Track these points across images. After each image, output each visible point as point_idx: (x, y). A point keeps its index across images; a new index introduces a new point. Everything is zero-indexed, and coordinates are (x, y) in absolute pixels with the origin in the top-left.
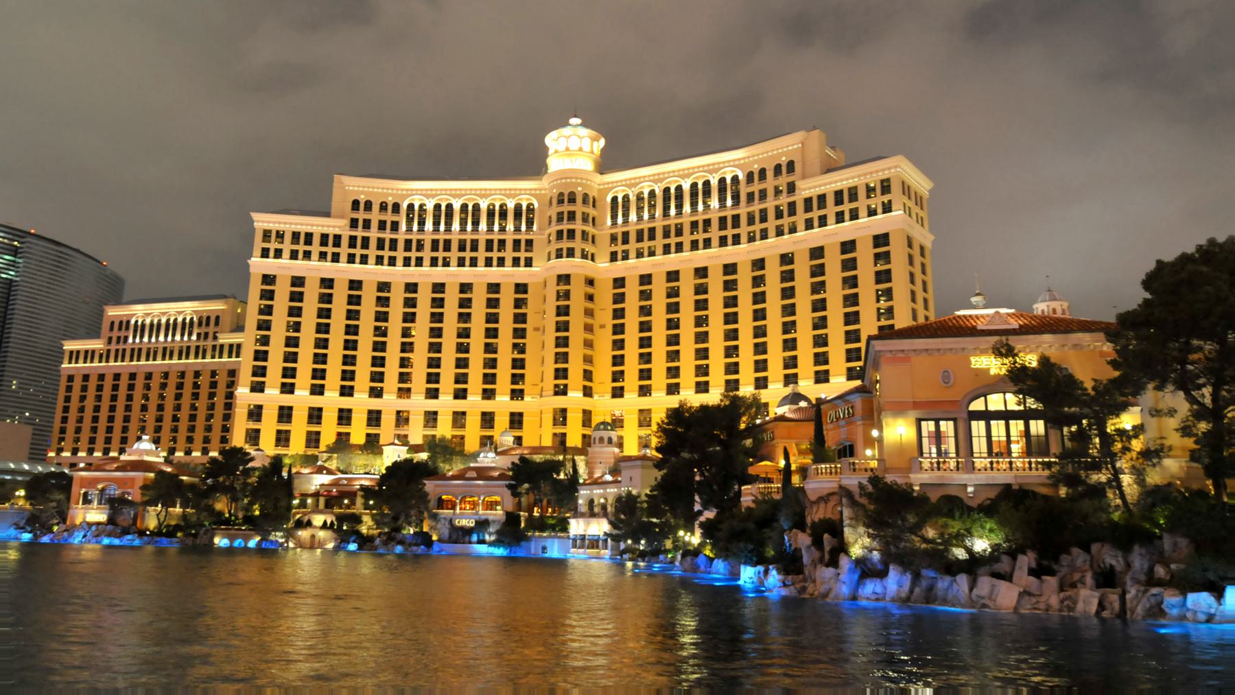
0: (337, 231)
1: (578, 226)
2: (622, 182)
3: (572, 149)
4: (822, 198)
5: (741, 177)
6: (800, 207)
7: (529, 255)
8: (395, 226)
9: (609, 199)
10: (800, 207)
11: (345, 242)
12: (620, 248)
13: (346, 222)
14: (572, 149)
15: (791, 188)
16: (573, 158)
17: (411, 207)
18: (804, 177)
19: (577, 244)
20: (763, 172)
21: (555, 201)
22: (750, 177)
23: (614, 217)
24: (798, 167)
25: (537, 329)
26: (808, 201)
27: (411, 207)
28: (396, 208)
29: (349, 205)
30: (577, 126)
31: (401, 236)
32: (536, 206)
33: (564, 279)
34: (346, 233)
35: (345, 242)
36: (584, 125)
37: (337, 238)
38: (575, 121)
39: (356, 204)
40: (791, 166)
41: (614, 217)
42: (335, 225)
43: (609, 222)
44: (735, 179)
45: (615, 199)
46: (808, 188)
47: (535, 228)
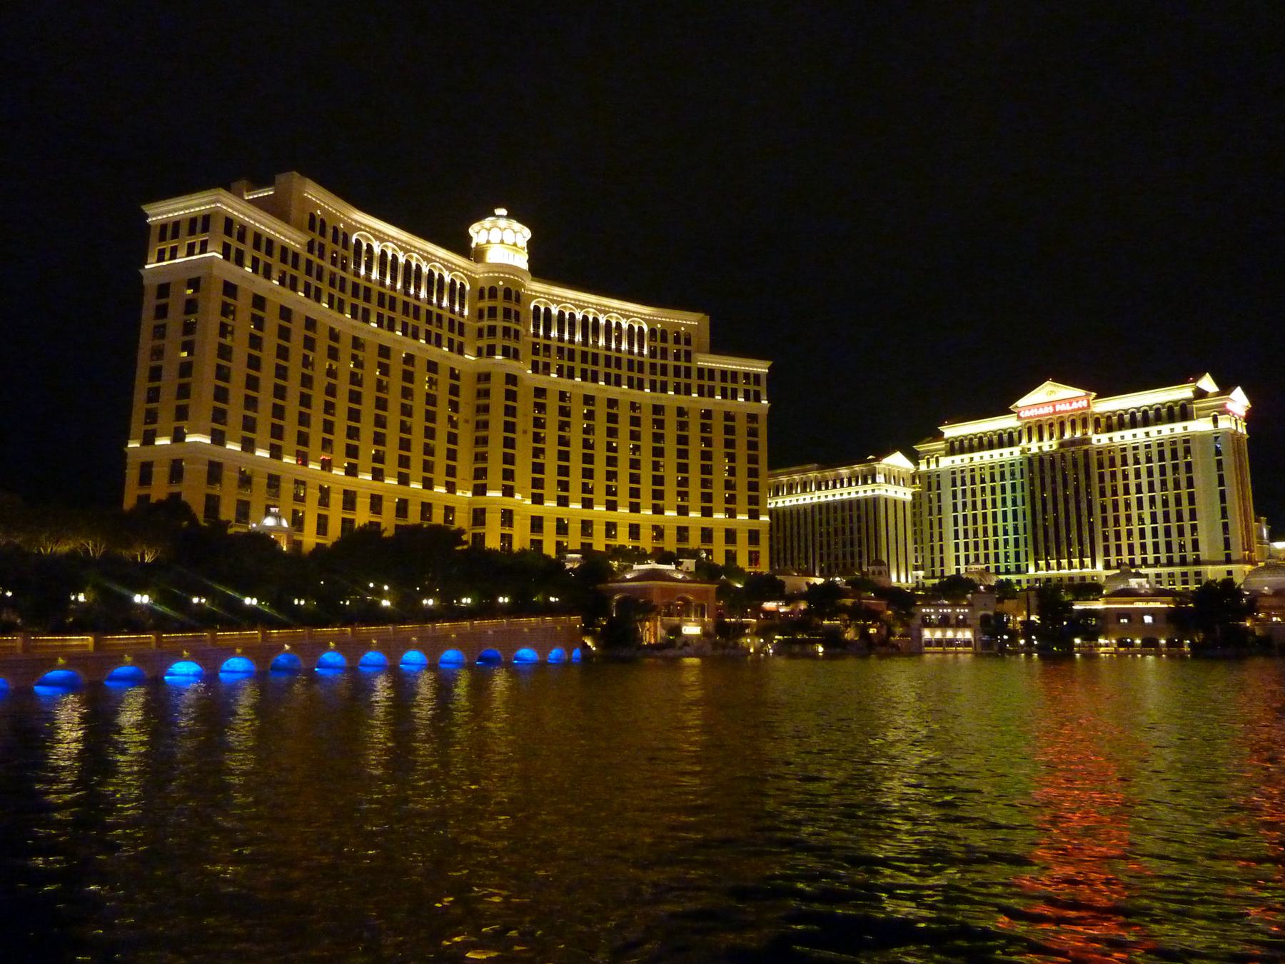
1: (500, 323)
2: (543, 294)
3: (503, 241)
4: (711, 371)
6: (694, 374)
7: (461, 339)
9: (532, 308)
10: (694, 374)
12: (541, 359)
13: (305, 239)
14: (503, 241)
15: (688, 356)
17: (358, 242)
18: (700, 351)
19: (499, 341)
20: (664, 333)
21: (500, 294)
22: (653, 332)
23: (536, 327)
24: (694, 340)
25: (467, 421)
26: (701, 370)
28: (346, 238)
29: (307, 218)
30: (499, 217)
32: (468, 288)
33: (511, 379)
34: (305, 255)
35: (302, 265)
36: (509, 216)
37: (296, 256)
38: (501, 211)
41: (536, 327)
42: (293, 239)
43: (532, 330)
44: (641, 329)
45: (537, 309)
46: (706, 361)
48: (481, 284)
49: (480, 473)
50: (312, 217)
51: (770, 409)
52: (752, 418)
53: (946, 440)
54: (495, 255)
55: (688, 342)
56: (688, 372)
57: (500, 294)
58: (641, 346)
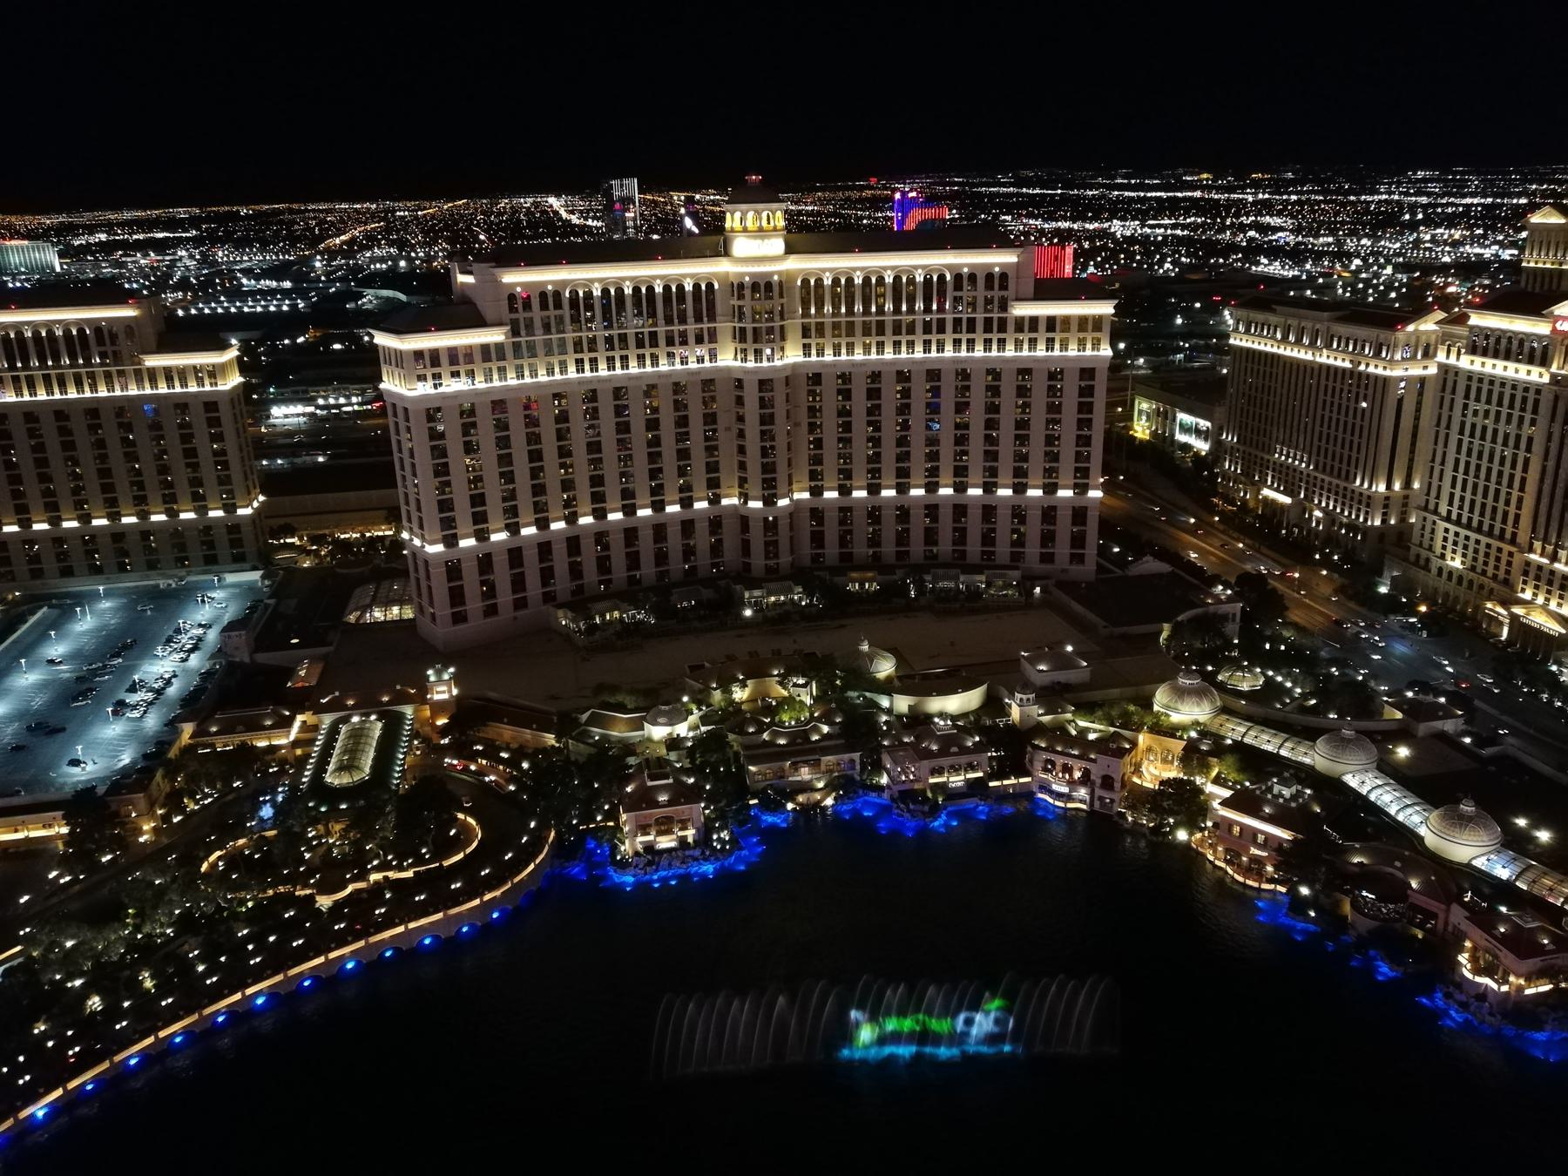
4: (1034, 321)
5: (948, 277)
10: (1011, 327)
15: (1004, 307)
18: (1018, 299)
20: (972, 277)
21: (747, 292)
22: (958, 278)
25: (728, 429)
40: (1004, 276)
46: (1022, 310)
50: (512, 298)
51: (1113, 357)
52: (1087, 373)
53: (1472, 328)
54: (742, 246)
55: (1004, 286)
57: (747, 292)
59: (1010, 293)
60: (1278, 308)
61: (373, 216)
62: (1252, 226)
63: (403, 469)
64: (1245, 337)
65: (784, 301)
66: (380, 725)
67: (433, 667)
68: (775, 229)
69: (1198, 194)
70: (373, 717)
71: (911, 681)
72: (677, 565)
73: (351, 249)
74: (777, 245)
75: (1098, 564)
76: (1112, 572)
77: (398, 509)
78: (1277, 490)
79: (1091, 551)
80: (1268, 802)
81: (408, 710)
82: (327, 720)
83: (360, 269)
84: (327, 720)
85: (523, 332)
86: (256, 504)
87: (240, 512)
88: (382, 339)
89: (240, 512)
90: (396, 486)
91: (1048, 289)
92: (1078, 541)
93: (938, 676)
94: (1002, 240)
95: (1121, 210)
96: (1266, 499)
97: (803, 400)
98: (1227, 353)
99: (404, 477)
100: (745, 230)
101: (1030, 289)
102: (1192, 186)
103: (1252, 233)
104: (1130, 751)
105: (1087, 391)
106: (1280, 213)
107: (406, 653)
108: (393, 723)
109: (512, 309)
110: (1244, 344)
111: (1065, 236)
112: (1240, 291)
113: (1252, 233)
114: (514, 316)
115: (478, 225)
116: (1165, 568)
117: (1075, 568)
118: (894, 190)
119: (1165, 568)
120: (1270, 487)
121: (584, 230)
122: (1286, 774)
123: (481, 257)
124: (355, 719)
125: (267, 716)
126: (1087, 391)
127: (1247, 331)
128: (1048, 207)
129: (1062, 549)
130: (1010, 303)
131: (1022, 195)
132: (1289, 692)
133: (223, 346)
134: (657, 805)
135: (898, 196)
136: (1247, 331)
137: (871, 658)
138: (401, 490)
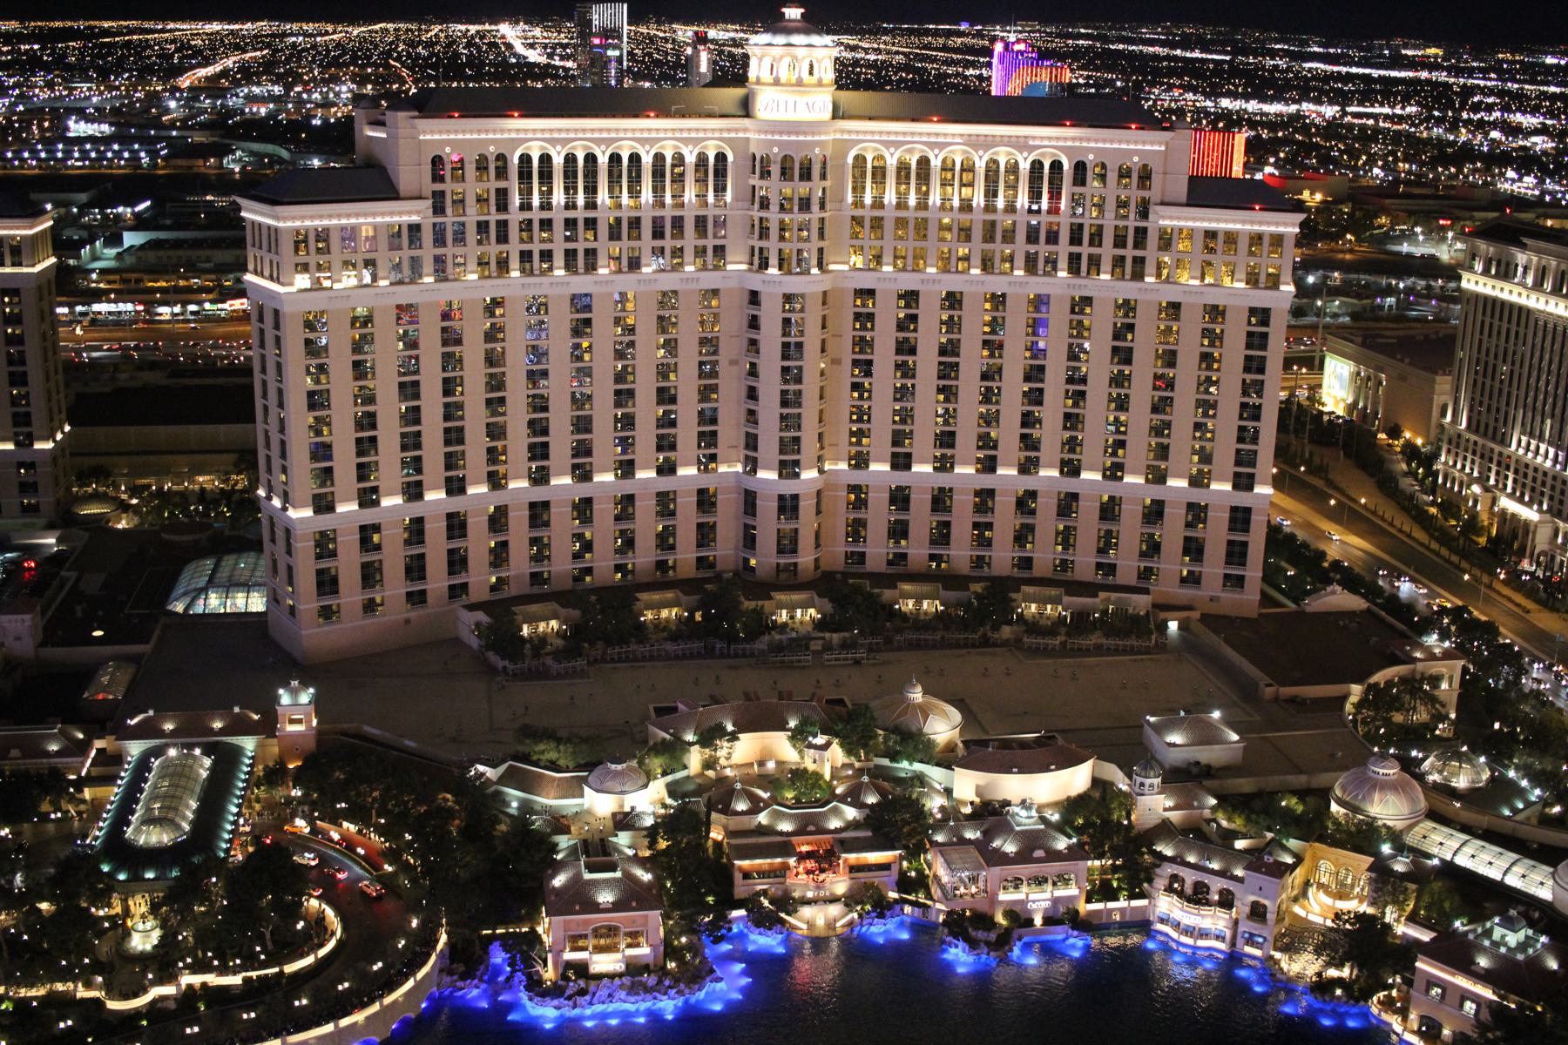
0: (415, 218)
5: (1066, 166)
8: (502, 196)
9: (850, 160)
10: (1152, 240)
11: (427, 236)
16: (810, 98)
17: (525, 159)
22: (1080, 168)
23: (858, 189)
24: (1156, 180)
25: (733, 362)
27: (525, 159)
29: (427, 168)
31: (515, 216)
32: (730, 158)
35: (427, 236)
37: (415, 229)
39: (437, 161)
40: (1145, 176)
43: (850, 199)
47: (729, 197)
48: (753, 149)
49: (752, 442)
50: (437, 161)
52: (1262, 315)
54: (771, 104)
56: (1141, 233)
58: (1055, 195)
59: (1154, 194)
60: (1525, 240)
61: (257, 41)
62: (1494, 125)
63: (265, 396)
64: (1482, 280)
65: (827, 184)
66: (207, 762)
67: (286, 685)
68: (820, 84)
69: (1424, 75)
70: (197, 752)
71: (977, 752)
72: (645, 556)
73: (212, 87)
74: (817, 104)
75: (1263, 593)
76: (1283, 606)
77: (254, 452)
78: (1520, 500)
79: (1253, 571)
80: (1484, 950)
81: (249, 744)
82: (135, 748)
83: (231, 113)
84: (135, 748)
85: (449, 211)
86: (59, 436)
87: (38, 446)
88: (253, 213)
89: (38, 446)
90: (253, 420)
91: (1208, 191)
92: (1236, 553)
93: (1024, 745)
94: (1150, 121)
95: (1308, 89)
96: (1503, 512)
97: (847, 329)
98: (1455, 300)
99: (266, 408)
100: (777, 82)
101: (1181, 190)
102: (1413, 64)
103: (1495, 134)
104: (1292, 868)
105: (1257, 341)
106: (1534, 111)
107: (249, 659)
108: (226, 759)
109: (437, 178)
110: (1480, 289)
111: (1232, 121)
112: (1476, 214)
113: (1495, 134)
114: (439, 187)
115: (398, 59)
116: (1355, 602)
117: (1229, 596)
118: (993, 40)
119: (1355, 602)
120: (1511, 496)
121: (545, 71)
122: (1513, 912)
123: (399, 102)
124: (172, 752)
125: (52, 737)
126: (1257, 341)
127: (1486, 272)
128: (1211, 80)
129: (1214, 566)
130: (1153, 209)
131: (1176, 59)
132: (1522, 793)
133: (36, 213)
134: (595, 908)
135: (999, 47)
136: (1486, 272)
137: (925, 712)
138: (260, 426)
